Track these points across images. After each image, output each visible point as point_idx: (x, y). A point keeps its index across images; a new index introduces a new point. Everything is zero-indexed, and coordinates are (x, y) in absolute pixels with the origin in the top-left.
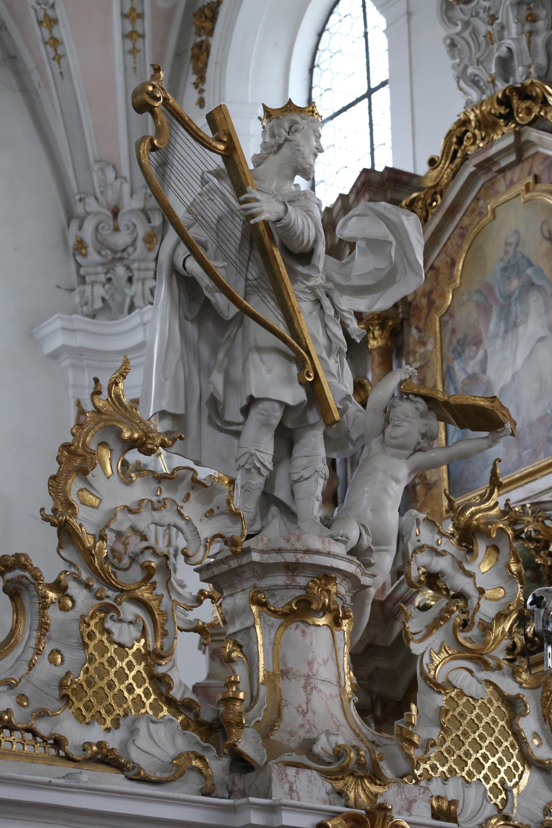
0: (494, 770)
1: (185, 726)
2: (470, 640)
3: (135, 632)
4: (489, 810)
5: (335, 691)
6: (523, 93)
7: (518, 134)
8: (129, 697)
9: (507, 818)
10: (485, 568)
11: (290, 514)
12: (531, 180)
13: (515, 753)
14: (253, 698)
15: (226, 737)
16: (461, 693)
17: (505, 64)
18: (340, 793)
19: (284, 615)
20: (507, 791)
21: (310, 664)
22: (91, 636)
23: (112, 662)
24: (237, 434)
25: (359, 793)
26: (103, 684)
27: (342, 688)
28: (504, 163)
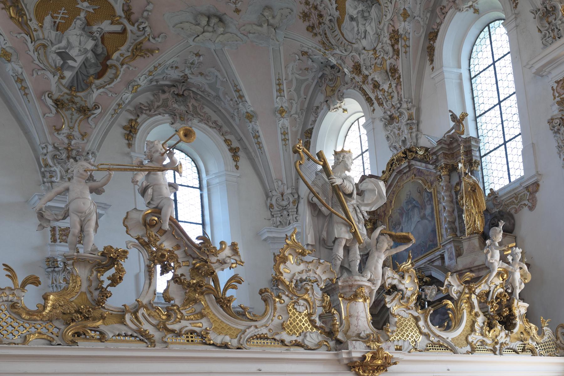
0: (412, 337)
1: (321, 333)
2: (404, 302)
3: (304, 308)
4: (411, 347)
5: (366, 320)
6: (410, 150)
7: (409, 162)
8: (303, 327)
9: (416, 349)
10: (408, 282)
11: (349, 271)
12: (413, 176)
13: (418, 331)
14: (341, 323)
15: (334, 335)
16: (402, 317)
17: (404, 142)
18: (369, 347)
19: (349, 300)
20: (416, 342)
21: (358, 313)
22: (290, 310)
23: (297, 317)
24: (332, 249)
25: (374, 346)
26: (295, 324)
27: (367, 319)
28: (405, 171)
